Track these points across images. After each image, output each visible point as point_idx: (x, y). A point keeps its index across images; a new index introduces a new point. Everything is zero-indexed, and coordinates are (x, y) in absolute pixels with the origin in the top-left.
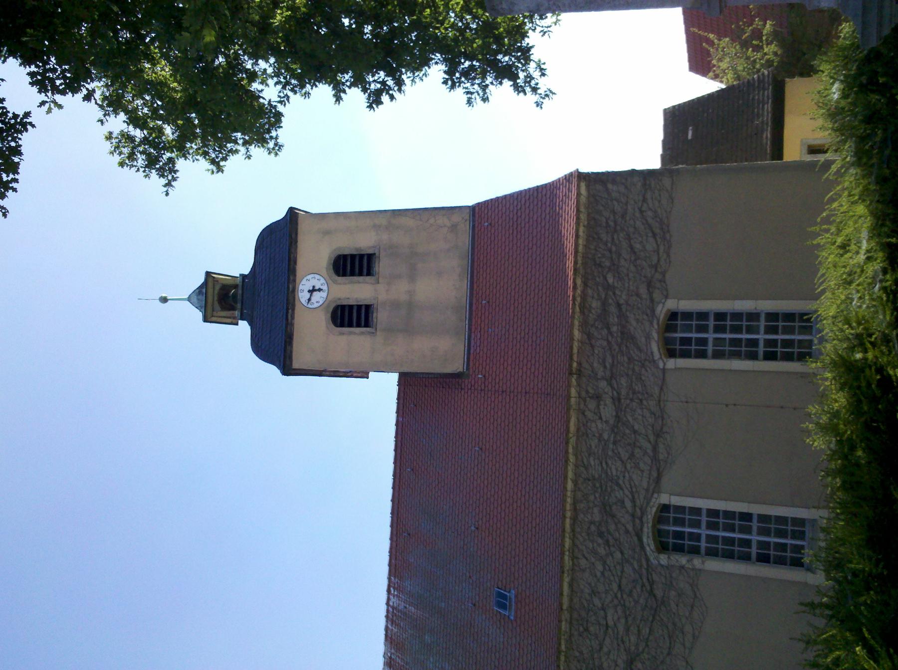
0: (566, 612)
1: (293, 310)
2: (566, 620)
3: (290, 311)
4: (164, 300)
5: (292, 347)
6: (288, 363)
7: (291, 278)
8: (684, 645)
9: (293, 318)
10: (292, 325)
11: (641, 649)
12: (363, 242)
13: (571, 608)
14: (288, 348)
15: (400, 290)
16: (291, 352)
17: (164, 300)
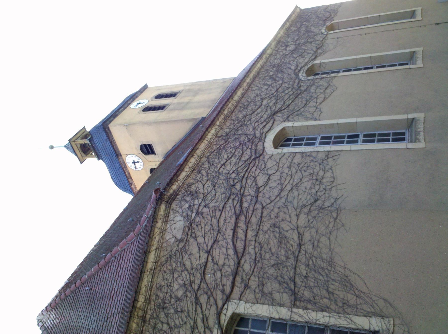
0: (234, 102)
1: (124, 109)
2: (233, 104)
3: (122, 109)
4: (52, 147)
5: (114, 119)
6: (108, 122)
7: (131, 100)
8: (317, 102)
9: (122, 111)
10: (120, 113)
11: (283, 109)
12: (174, 90)
13: (239, 102)
14: (112, 119)
15: (186, 100)
16: (112, 120)
17: (52, 147)
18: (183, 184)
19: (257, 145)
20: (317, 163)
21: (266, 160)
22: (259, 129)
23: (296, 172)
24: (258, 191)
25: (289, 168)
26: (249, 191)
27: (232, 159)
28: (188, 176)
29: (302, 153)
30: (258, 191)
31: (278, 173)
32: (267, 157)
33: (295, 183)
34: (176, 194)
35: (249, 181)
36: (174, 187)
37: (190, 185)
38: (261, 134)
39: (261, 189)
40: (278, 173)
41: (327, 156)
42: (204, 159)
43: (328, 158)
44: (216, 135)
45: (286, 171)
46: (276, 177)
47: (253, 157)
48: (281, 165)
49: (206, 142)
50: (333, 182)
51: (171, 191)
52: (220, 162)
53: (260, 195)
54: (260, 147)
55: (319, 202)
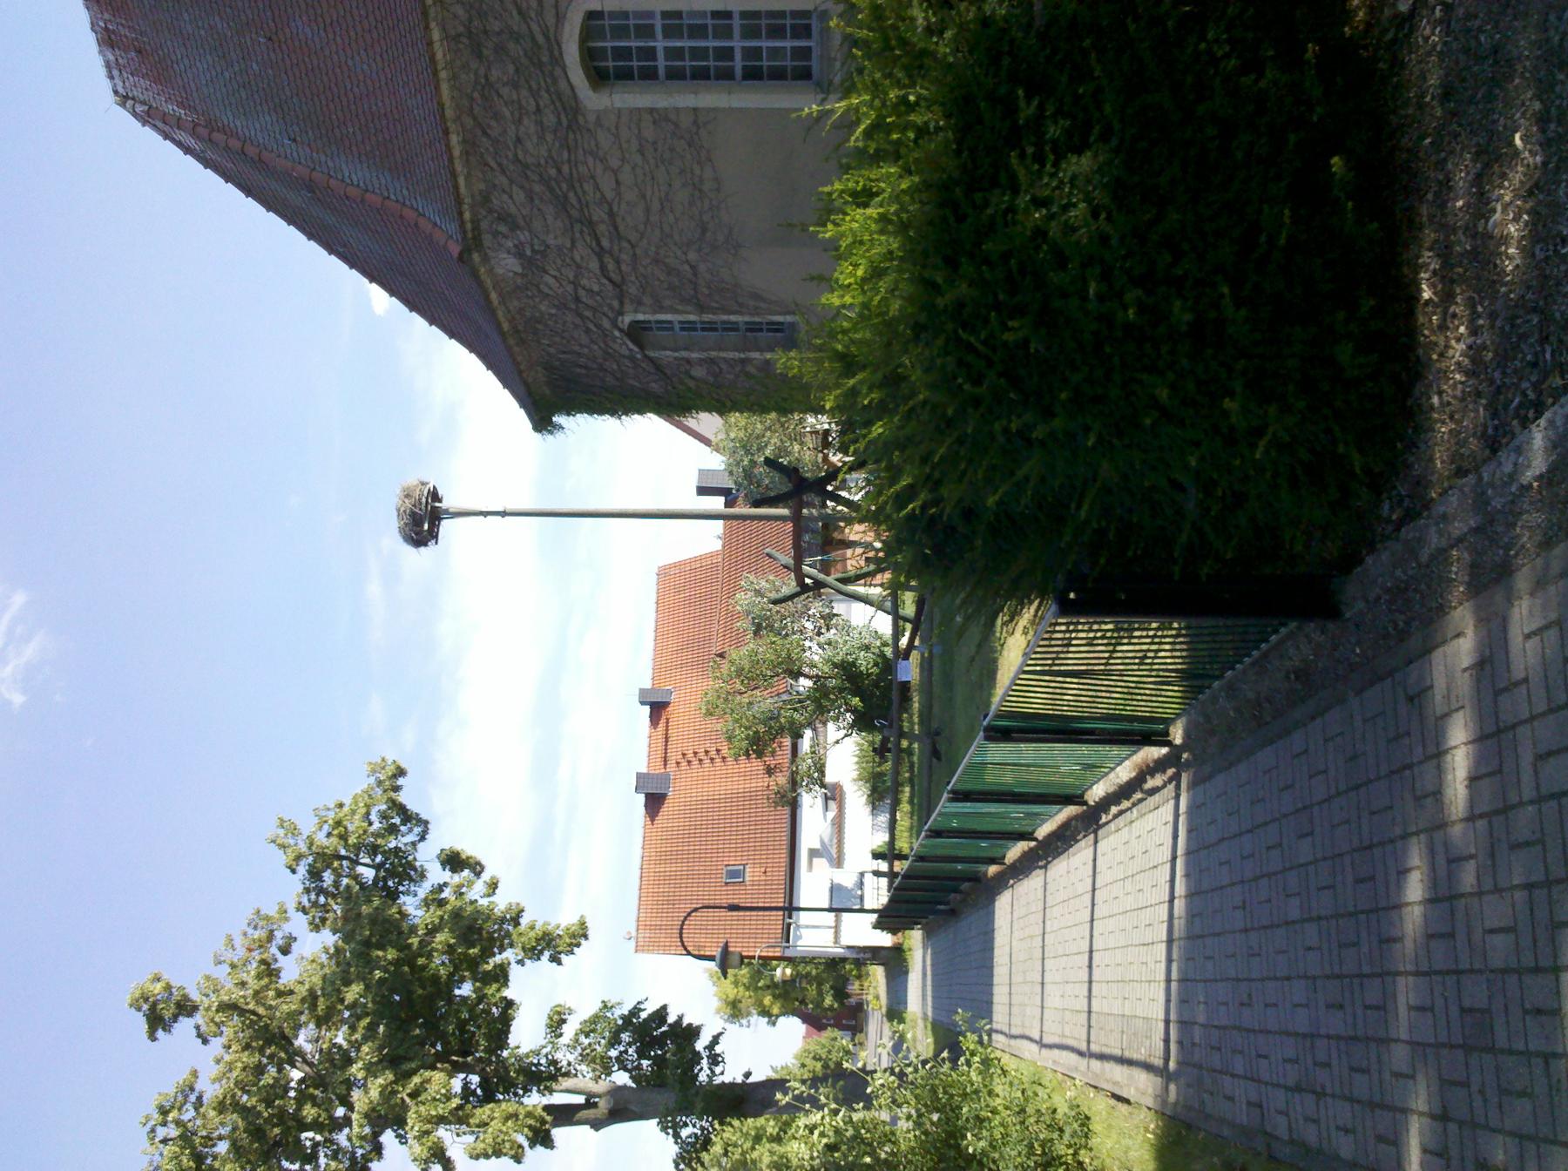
18: (473, 196)
19: (555, 81)
20: (683, 141)
21: (591, 126)
22: (533, 15)
23: (657, 166)
24: (611, 214)
25: (641, 152)
26: (599, 214)
27: (526, 121)
28: (468, 177)
29: (651, 111)
30: (611, 214)
31: (627, 168)
32: (592, 118)
33: (663, 194)
34: (476, 223)
35: (586, 187)
36: (467, 216)
37: (486, 199)
38: (547, 38)
39: (615, 209)
40: (627, 168)
41: (695, 122)
42: (469, 122)
43: (699, 128)
44: (446, 37)
45: (638, 159)
46: (626, 176)
47: (565, 122)
48: (625, 146)
49: (443, 75)
50: (718, 190)
51: (469, 226)
52: (505, 131)
53: (619, 220)
54: (563, 85)
55: (708, 234)
